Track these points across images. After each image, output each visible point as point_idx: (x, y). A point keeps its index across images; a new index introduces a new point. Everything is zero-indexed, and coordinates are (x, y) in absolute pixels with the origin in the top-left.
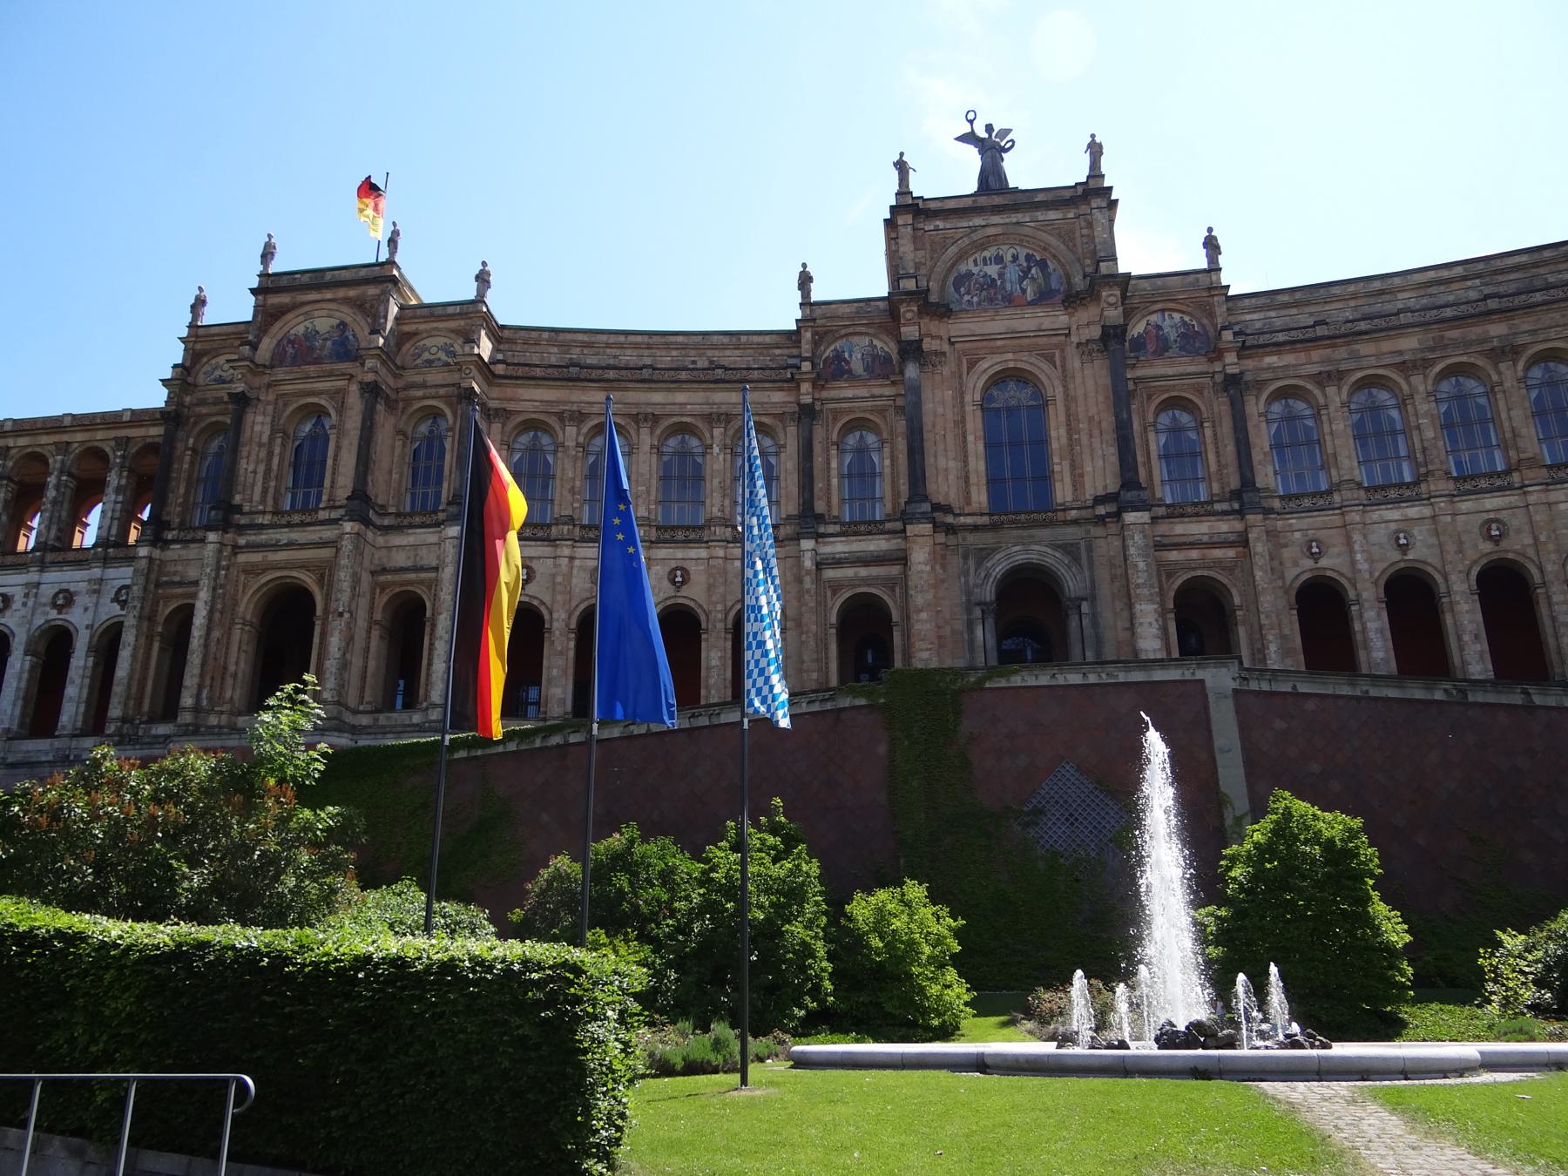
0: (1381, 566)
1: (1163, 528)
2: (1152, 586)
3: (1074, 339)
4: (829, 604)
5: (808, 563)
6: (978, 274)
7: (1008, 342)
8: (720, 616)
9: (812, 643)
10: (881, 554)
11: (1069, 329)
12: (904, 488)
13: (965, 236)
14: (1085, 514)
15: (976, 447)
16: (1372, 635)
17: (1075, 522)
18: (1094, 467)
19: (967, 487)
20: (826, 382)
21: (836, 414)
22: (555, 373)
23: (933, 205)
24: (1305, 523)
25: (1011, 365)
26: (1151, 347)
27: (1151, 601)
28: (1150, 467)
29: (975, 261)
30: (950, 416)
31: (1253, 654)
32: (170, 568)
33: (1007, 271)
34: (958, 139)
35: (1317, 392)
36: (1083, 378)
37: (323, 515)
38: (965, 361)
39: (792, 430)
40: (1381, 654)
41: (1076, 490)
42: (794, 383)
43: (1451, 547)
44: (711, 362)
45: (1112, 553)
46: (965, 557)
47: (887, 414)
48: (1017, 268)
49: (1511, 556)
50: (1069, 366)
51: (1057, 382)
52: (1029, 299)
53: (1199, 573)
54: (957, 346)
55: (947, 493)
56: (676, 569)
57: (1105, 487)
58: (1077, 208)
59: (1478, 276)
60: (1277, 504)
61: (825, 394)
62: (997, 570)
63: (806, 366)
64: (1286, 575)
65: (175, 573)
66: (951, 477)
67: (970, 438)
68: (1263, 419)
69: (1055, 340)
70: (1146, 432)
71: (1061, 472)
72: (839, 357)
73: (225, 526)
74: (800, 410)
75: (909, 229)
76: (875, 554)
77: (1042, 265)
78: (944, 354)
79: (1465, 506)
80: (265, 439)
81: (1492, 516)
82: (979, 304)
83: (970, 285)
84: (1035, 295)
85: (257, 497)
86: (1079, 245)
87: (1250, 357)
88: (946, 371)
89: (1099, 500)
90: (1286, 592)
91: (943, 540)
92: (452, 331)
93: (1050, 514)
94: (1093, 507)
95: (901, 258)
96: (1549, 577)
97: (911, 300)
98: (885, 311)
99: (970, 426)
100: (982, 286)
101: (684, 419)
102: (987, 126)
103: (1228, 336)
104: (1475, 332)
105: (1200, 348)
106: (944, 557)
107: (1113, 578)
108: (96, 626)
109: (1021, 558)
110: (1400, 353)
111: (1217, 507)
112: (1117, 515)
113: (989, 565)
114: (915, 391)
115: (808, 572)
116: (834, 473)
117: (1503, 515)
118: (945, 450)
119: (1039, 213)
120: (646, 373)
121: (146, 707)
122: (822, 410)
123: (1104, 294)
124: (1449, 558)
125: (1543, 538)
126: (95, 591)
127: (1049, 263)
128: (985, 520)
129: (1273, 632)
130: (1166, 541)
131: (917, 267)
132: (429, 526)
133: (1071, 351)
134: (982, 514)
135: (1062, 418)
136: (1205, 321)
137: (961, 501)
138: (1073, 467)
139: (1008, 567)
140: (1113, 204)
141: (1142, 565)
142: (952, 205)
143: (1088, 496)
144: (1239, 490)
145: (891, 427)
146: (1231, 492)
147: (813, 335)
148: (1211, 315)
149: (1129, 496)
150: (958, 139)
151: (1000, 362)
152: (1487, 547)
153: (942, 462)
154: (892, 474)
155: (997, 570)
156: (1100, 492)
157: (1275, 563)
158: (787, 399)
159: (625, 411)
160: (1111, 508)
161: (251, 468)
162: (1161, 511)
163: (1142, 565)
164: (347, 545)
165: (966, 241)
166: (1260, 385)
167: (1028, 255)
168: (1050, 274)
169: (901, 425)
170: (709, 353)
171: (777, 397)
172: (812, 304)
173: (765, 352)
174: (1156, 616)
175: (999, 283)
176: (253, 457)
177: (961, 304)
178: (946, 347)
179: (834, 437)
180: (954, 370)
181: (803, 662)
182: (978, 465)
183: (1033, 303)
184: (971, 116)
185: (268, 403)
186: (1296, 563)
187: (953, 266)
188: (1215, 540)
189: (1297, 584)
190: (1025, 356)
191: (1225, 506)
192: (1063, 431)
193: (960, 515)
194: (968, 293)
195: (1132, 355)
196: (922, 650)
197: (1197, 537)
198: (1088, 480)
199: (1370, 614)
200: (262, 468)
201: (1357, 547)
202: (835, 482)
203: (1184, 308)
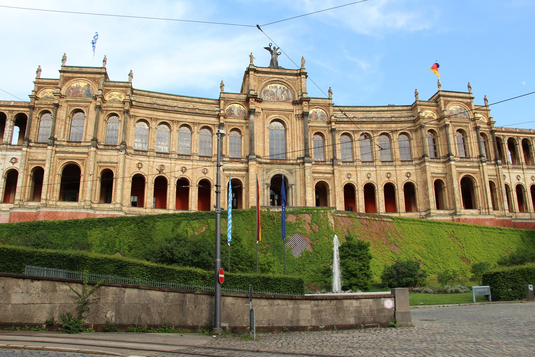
0: (363, 182)
4: (226, 181)
8: (195, 182)
14: (295, 162)
15: (267, 140)
16: (360, 199)
17: (292, 164)
21: (229, 126)
22: (149, 106)
23: (259, 69)
24: (347, 169)
25: (278, 118)
26: (314, 118)
32: (32, 155)
33: (278, 91)
35: (352, 135)
37: (82, 144)
40: (362, 204)
42: (218, 117)
43: (379, 178)
44: (194, 106)
46: (263, 171)
49: (391, 182)
50: (293, 120)
51: (289, 124)
53: (322, 180)
56: (183, 167)
59: (391, 111)
61: (226, 120)
65: (34, 156)
66: (260, 148)
67: (266, 137)
72: (230, 109)
73: (53, 145)
77: (288, 91)
79: (383, 169)
80: (64, 118)
81: (388, 172)
82: (270, 99)
85: (62, 136)
87: (337, 124)
89: (298, 158)
92: (122, 90)
96: (399, 188)
97: (253, 97)
99: (266, 134)
101: (186, 123)
103: (333, 118)
104: (388, 125)
108: (4, 170)
109: (278, 173)
110: (372, 128)
111: (327, 163)
112: (303, 163)
114: (253, 123)
116: (228, 143)
117: (390, 172)
120: (176, 109)
121: (26, 197)
124: (378, 181)
125: (398, 178)
126: (4, 159)
128: (268, 161)
132: (113, 150)
133: (293, 116)
135: (290, 135)
136: (327, 113)
140: (307, 77)
141: (309, 177)
148: (329, 111)
149: (306, 159)
152: (387, 179)
153: (258, 144)
156: (299, 156)
157: (340, 179)
159: (170, 119)
160: (301, 161)
161: (60, 127)
163: (309, 177)
164: (92, 154)
165: (268, 81)
170: (193, 103)
171: (213, 119)
172: (224, 93)
176: (60, 124)
178: (260, 111)
182: (267, 145)
183: (284, 101)
184: (270, 45)
185: (65, 107)
186: (344, 179)
187: (264, 87)
188: (326, 172)
189: (344, 185)
190: (281, 116)
191: (329, 163)
192: (290, 138)
194: (267, 96)
199: (360, 194)
200: (63, 127)
201: (359, 176)
202: (228, 146)
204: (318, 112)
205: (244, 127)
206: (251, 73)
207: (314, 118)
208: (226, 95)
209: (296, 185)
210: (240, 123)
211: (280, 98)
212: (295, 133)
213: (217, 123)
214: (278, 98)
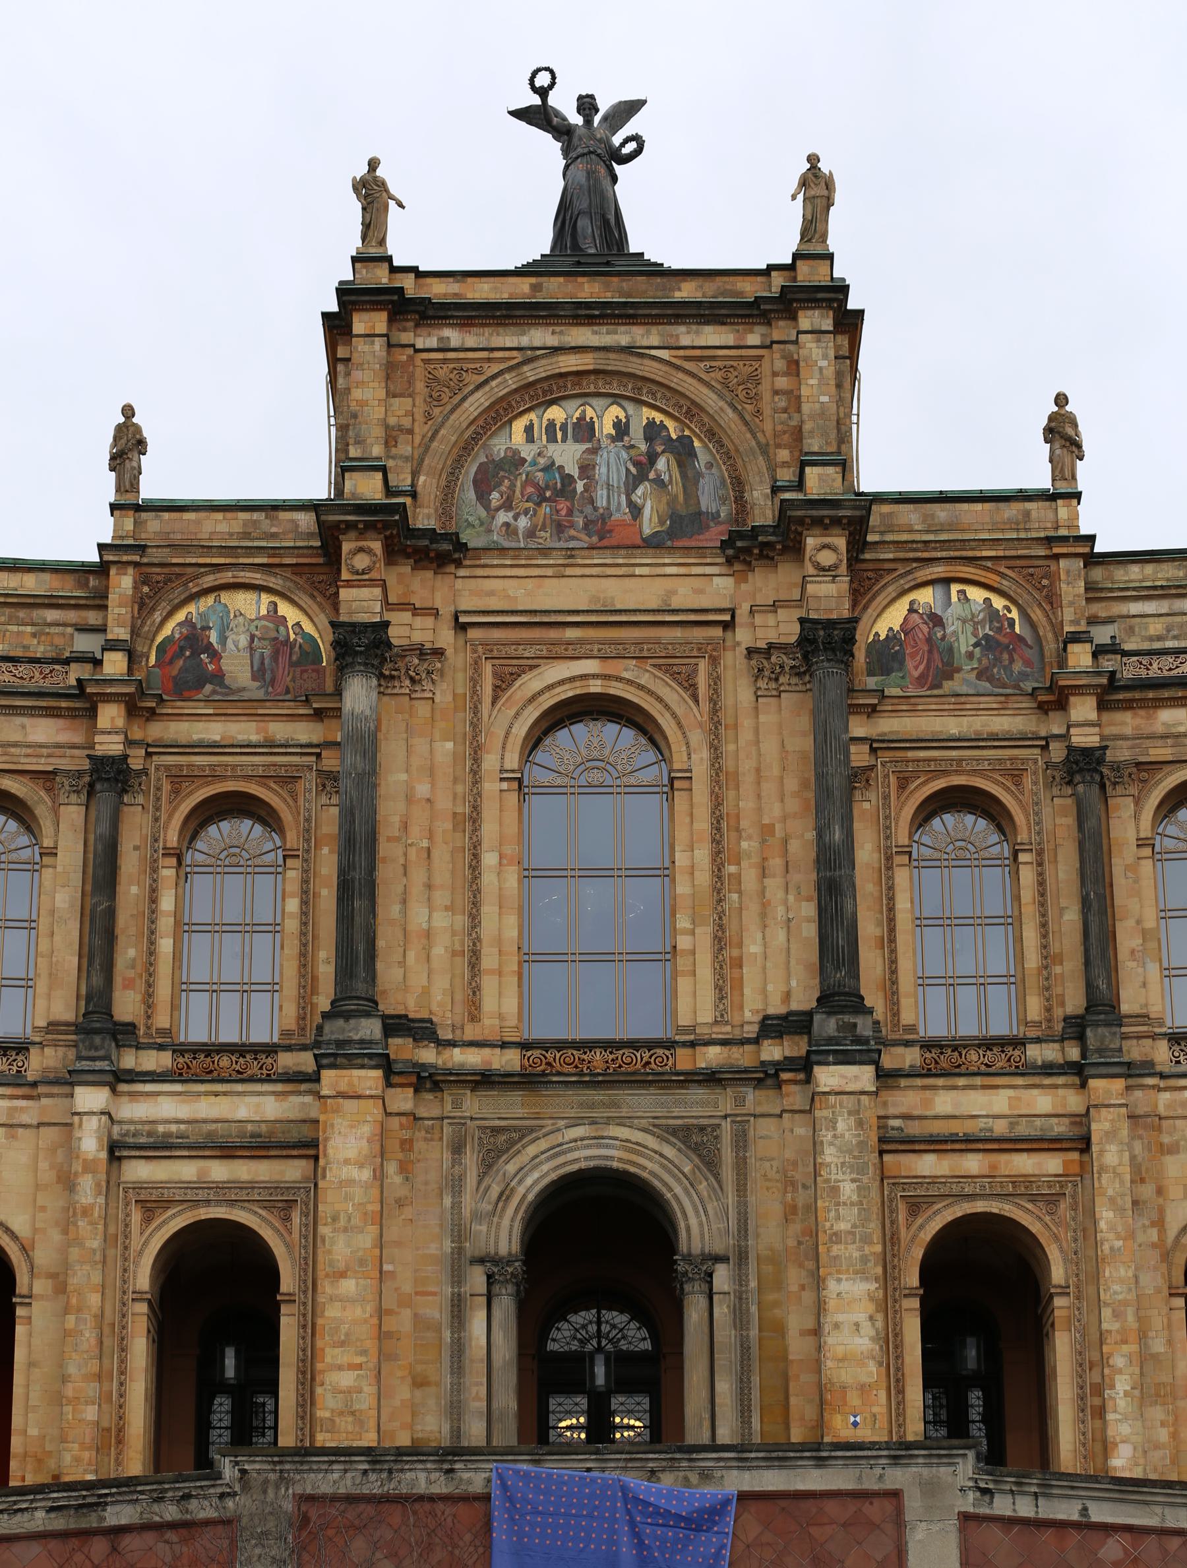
1: (906, 1100)
2: (866, 1240)
3: (743, 636)
4: (136, 1242)
5: (90, 1143)
6: (534, 463)
7: (591, 633)
9: (89, 1336)
10: (264, 1128)
11: (733, 612)
12: (326, 969)
13: (510, 369)
14: (742, 1057)
17: (712, 1078)
18: (765, 945)
19: (473, 976)
20: (161, 700)
21: (180, 780)
23: (438, 290)
25: (596, 687)
26: (914, 668)
27: (862, 1274)
28: (893, 951)
29: (529, 429)
30: (444, 803)
31: (1082, 1398)
34: (512, 113)
36: (757, 730)
38: (488, 669)
39: (73, 814)
41: (721, 998)
45: (789, 1154)
46: (457, 1149)
47: (300, 786)
48: (624, 455)
50: (727, 700)
51: (697, 737)
52: (647, 531)
53: (980, 1206)
54: (473, 634)
55: (426, 992)
57: (787, 996)
58: (769, 324)
60: (1162, 1053)
61: (157, 731)
62: (529, 1181)
63: (114, 664)
64: (1168, 1218)
66: (438, 951)
67: (489, 859)
68: (1147, 851)
69: (699, 634)
70: (889, 868)
71: (693, 952)
74: (93, 771)
75: (379, 345)
76: (249, 1127)
77: (683, 451)
78: (439, 653)
82: (531, 533)
83: (512, 488)
84: (662, 523)
86: (767, 411)
87: (1128, 706)
88: (443, 694)
90: (1166, 1256)
91: (408, 1106)
93: (660, 1052)
94: (756, 1041)
95: (355, 416)
97: (369, 526)
98: (310, 535)
99: (489, 829)
100: (541, 491)
102: (580, 98)
105: (1024, 676)
106: (407, 1145)
107: (790, 1212)
109: (582, 1158)
111: (1036, 1053)
112: (805, 1066)
113: (511, 1168)
115: (89, 1167)
118: (429, 887)
119: (682, 329)
122: (145, 772)
123: (811, 542)
127: (697, 444)
128: (510, 1060)
129: (1125, 1348)
130: (914, 1129)
131: (391, 438)
133: (734, 663)
134: (504, 1045)
135: (703, 824)
136: (1037, 615)
137: (459, 1009)
138: (720, 942)
139: (554, 1176)
141: (848, 1190)
142: (482, 292)
143: (750, 1015)
144: (1082, 1017)
145: (308, 820)
146: (1066, 1019)
147: (143, 580)
148: (1052, 599)
149: (827, 1026)
150: (512, 113)
151: (572, 679)
153: (419, 916)
154: (303, 934)
155: (529, 1181)
156: (776, 1008)
157: (1147, 1191)
158: (63, 738)
162: (910, 1057)
163: (848, 1190)
165: (511, 382)
166: (1147, 769)
167: (651, 424)
168: (699, 475)
169: (329, 820)
172: (138, 508)
173: (22, 614)
174: (871, 1308)
175: (580, 486)
177: (489, 531)
178: (446, 638)
179: (172, 837)
180: (460, 691)
181: (65, 1379)
183: (653, 544)
184: (543, 80)
188: (1023, 1130)
190: (628, 668)
192: (703, 855)
193: (452, 1044)
194: (507, 505)
195: (872, 682)
196: (340, 1368)
197: (982, 1123)
198: (750, 973)
203: (992, 579)
204: (953, 615)
205: (310, 781)
206: (360, 324)
207: (914, 668)
208: (154, 524)
209: (742, 1256)
210: (271, 746)
211: (622, 513)
212: (747, 805)
213: (77, 761)
214: (605, 517)
